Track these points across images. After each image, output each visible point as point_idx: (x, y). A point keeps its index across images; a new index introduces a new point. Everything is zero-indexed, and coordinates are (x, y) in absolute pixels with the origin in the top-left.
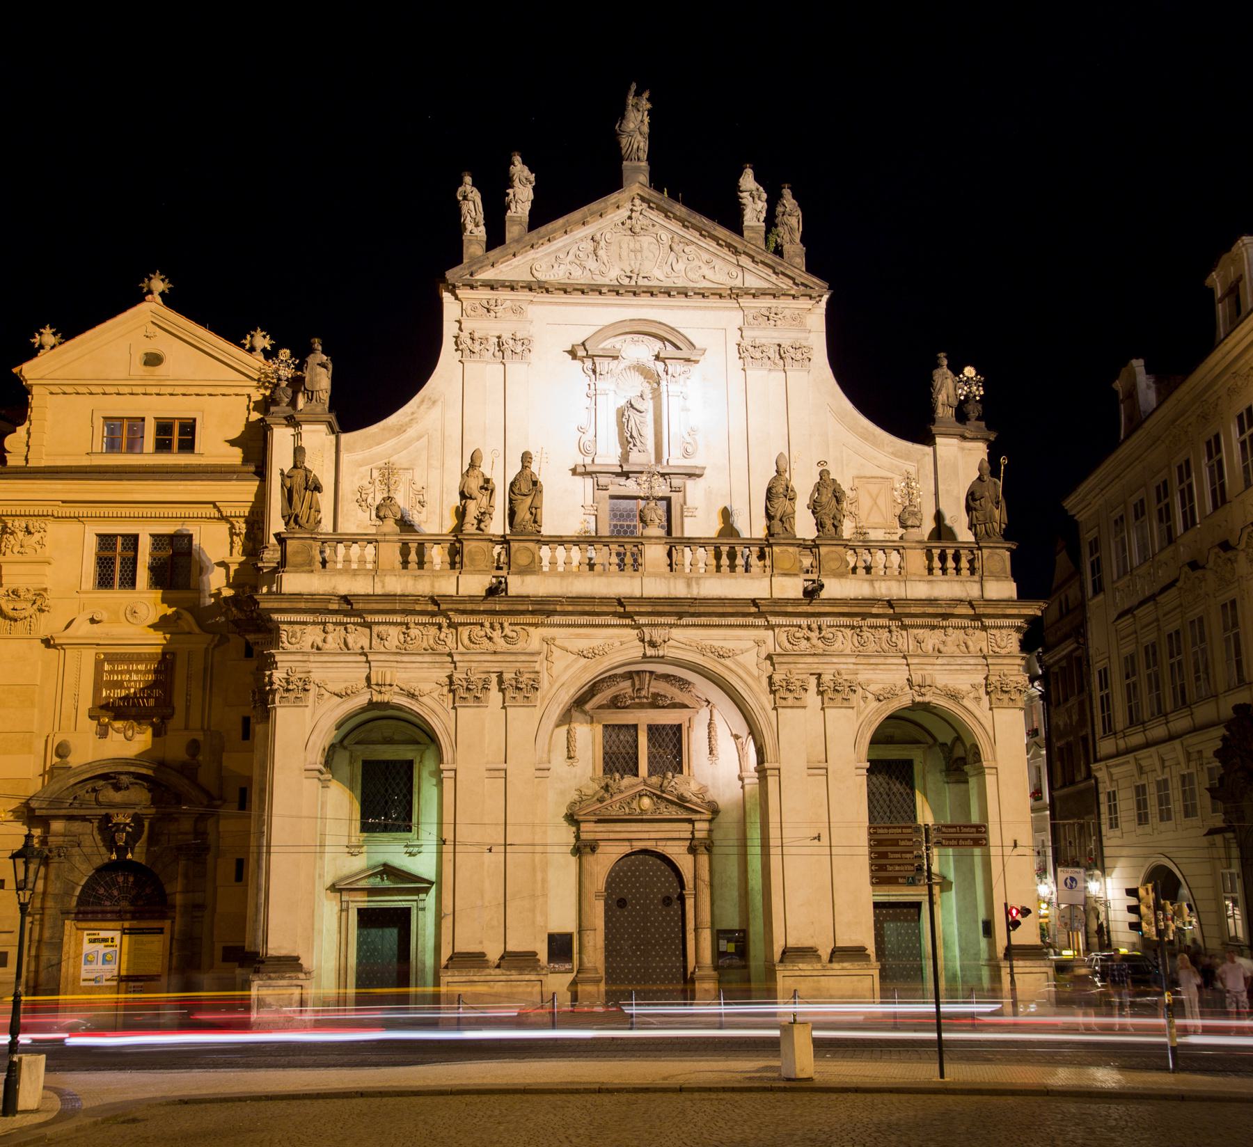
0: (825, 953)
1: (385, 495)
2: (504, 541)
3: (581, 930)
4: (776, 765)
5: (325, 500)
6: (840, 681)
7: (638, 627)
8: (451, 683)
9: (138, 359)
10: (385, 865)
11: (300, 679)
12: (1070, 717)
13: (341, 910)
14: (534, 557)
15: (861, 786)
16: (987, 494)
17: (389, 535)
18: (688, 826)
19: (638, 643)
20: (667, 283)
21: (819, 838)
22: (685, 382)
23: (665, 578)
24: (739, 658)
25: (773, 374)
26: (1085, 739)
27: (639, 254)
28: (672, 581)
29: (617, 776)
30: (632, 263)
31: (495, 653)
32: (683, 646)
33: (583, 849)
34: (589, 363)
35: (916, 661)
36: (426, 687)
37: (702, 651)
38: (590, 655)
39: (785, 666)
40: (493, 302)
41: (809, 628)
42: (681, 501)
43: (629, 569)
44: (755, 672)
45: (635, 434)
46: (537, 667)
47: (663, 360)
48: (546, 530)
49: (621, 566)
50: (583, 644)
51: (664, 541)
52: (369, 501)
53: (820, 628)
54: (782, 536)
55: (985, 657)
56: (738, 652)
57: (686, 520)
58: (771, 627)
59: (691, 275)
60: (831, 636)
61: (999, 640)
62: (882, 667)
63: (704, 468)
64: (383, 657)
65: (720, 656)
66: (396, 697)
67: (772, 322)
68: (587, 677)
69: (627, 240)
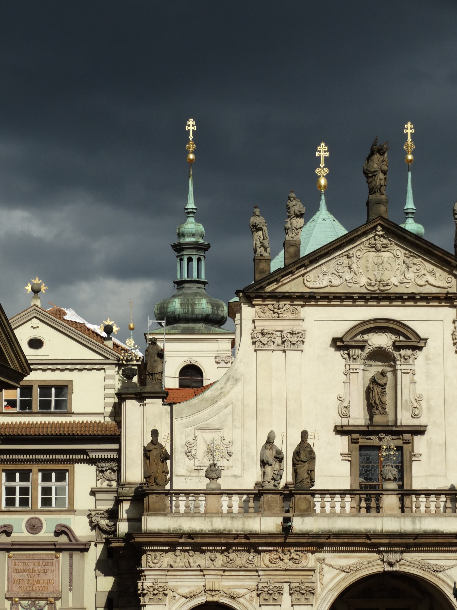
8: (258, 589)
11: (160, 587)
14: (310, 504)
20: (401, 290)
22: (413, 362)
23: (398, 517)
24: (448, 572)
27: (381, 266)
28: (402, 519)
30: (376, 273)
31: (286, 570)
32: (410, 564)
36: (242, 591)
38: (347, 570)
40: (276, 306)
42: (410, 449)
43: (373, 511)
45: (377, 402)
46: (313, 579)
47: (397, 348)
49: (368, 509)
51: (397, 492)
52: (193, 452)
56: (446, 568)
57: (414, 464)
63: (426, 426)
64: (214, 573)
65: (435, 571)
66: (221, 598)
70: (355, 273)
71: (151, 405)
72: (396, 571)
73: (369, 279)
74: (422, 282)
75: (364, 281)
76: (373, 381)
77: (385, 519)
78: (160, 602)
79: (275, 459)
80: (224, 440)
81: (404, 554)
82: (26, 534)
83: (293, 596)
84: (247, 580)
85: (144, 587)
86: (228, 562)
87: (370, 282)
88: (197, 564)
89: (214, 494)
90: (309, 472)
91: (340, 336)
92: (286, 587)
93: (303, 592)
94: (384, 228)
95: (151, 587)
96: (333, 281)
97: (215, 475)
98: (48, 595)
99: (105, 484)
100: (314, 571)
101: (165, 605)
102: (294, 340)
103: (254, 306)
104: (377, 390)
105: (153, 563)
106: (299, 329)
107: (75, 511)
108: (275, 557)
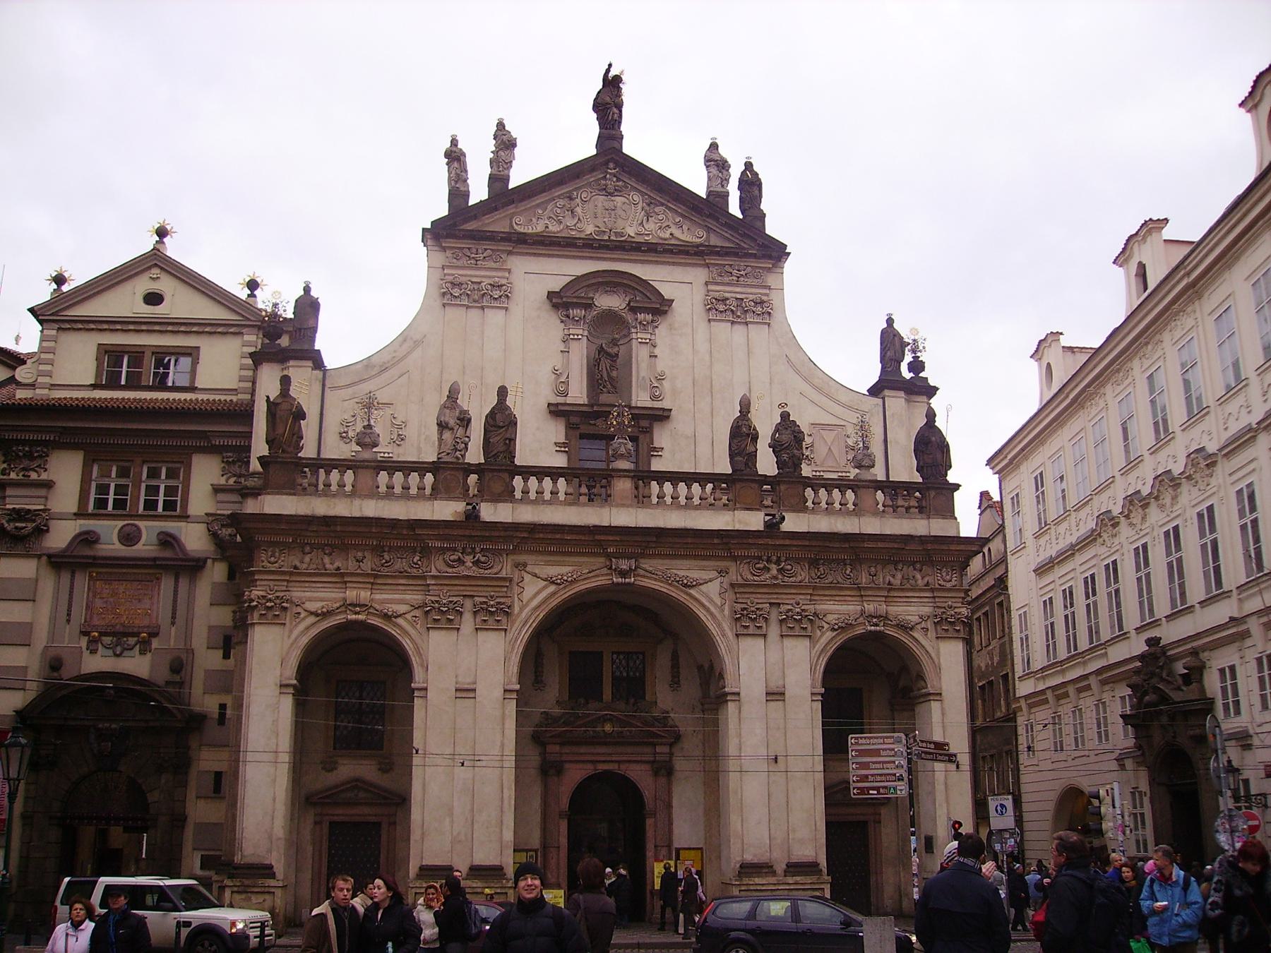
0: (780, 867)
1: (366, 423)
2: (477, 469)
3: (545, 846)
4: (737, 690)
5: (309, 428)
6: (798, 610)
7: (609, 556)
9: (140, 299)
10: (357, 780)
11: (278, 597)
12: (992, 659)
13: (316, 823)
15: (816, 710)
16: (933, 439)
17: (367, 461)
18: (648, 750)
19: (605, 571)
21: (776, 760)
24: (703, 588)
25: (736, 327)
26: (1005, 677)
29: (582, 701)
31: (468, 577)
33: (550, 770)
34: (562, 312)
35: (870, 593)
36: (402, 608)
37: (666, 580)
38: (559, 581)
39: (747, 596)
40: (474, 251)
41: (769, 561)
44: (718, 601)
45: (605, 375)
47: (633, 310)
48: (517, 462)
50: (553, 571)
53: (779, 558)
54: (744, 472)
55: (932, 590)
56: (701, 582)
58: (735, 559)
59: (662, 235)
60: (789, 567)
61: (944, 574)
62: (837, 598)
65: (686, 586)
67: (735, 278)
68: (554, 602)
69: (601, 200)
70: (579, 219)
71: (296, 369)
72: (629, 584)
73: (598, 227)
74: (667, 235)
75: (590, 229)
76: (601, 350)
77: (614, 510)
78: (276, 621)
79: (458, 422)
80: (394, 418)
81: (642, 561)
82: (118, 546)
83: (478, 617)
84: (410, 592)
85: (252, 597)
86: (382, 566)
87: (597, 229)
88: (336, 565)
89: (367, 467)
90: (507, 442)
91: (558, 290)
92: (468, 604)
93: (494, 609)
94: (617, 164)
95: (264, 597)
96: (550, 227)
97: (369, 440)
98: (141, 630)
99: (231, 481)
100: (511, 580)
101: (285, 624)
102: (496, 294)
103: (444, 249)
104: (605, 363)
105: (269, 562)
106: (503, 283)
107: (189, 517)
108: (452, 557)
